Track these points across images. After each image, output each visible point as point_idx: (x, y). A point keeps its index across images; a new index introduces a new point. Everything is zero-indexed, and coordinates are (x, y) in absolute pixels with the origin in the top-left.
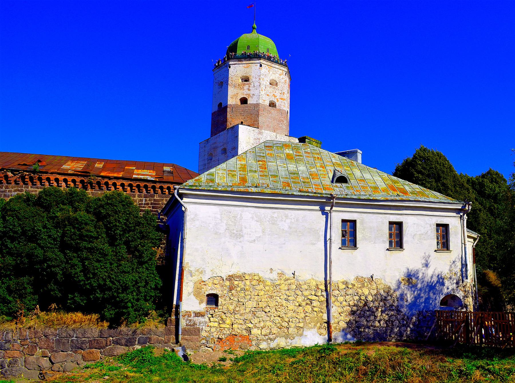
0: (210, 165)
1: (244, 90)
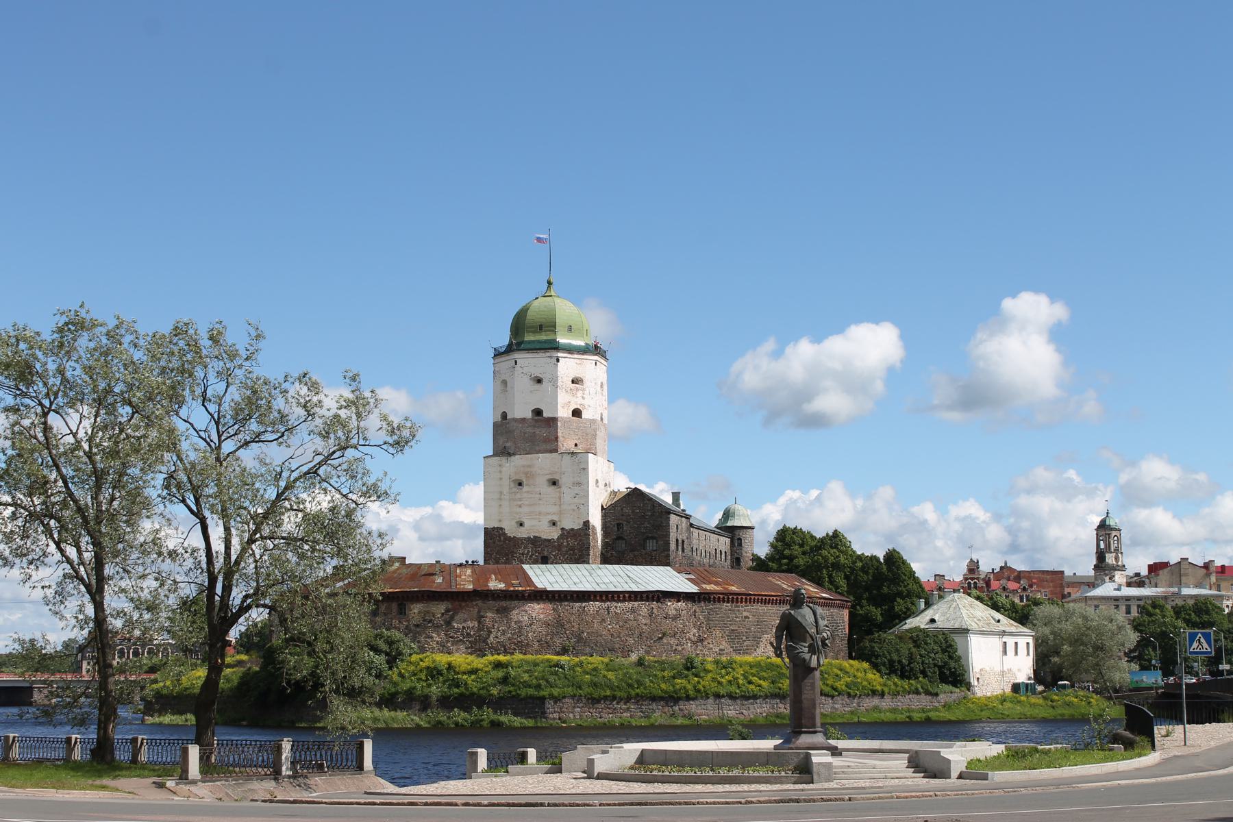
0: (518, 496)
1: (577, 397)
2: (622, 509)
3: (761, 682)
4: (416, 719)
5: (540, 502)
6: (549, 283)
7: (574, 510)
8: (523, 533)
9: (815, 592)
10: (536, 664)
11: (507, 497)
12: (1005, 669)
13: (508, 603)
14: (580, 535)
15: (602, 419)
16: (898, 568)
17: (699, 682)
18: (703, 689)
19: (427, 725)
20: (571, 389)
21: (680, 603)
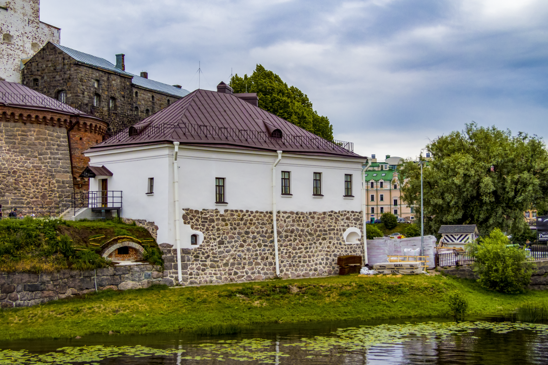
2: (38, 65)
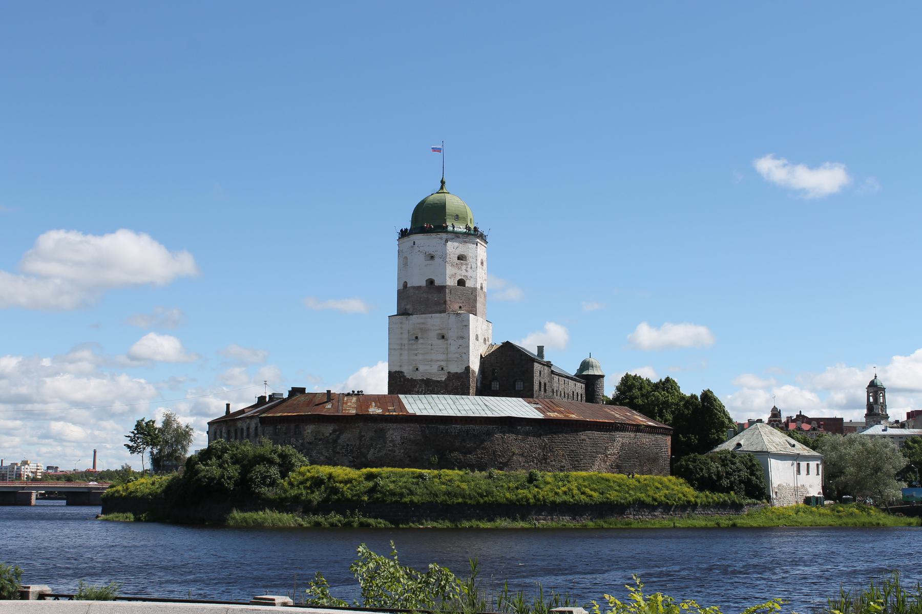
0: (415, 347)
3: (593, 493)
4: (300, 520)
5: (432, 351)
6: (443, 183)
7: (458, 358)
8: (418, 376)
9: (642, 421)
10: (402, 476)
11: (406, 347)
12: (799, 485)
13: (385, 425)
14: (462, 378)
15: (482, 288)
16: (712, 404)
17: (538, 492)
18: (542, 498)
19: (308, 525)
20: (457, 264)
21: (528, 428)
